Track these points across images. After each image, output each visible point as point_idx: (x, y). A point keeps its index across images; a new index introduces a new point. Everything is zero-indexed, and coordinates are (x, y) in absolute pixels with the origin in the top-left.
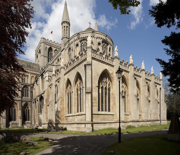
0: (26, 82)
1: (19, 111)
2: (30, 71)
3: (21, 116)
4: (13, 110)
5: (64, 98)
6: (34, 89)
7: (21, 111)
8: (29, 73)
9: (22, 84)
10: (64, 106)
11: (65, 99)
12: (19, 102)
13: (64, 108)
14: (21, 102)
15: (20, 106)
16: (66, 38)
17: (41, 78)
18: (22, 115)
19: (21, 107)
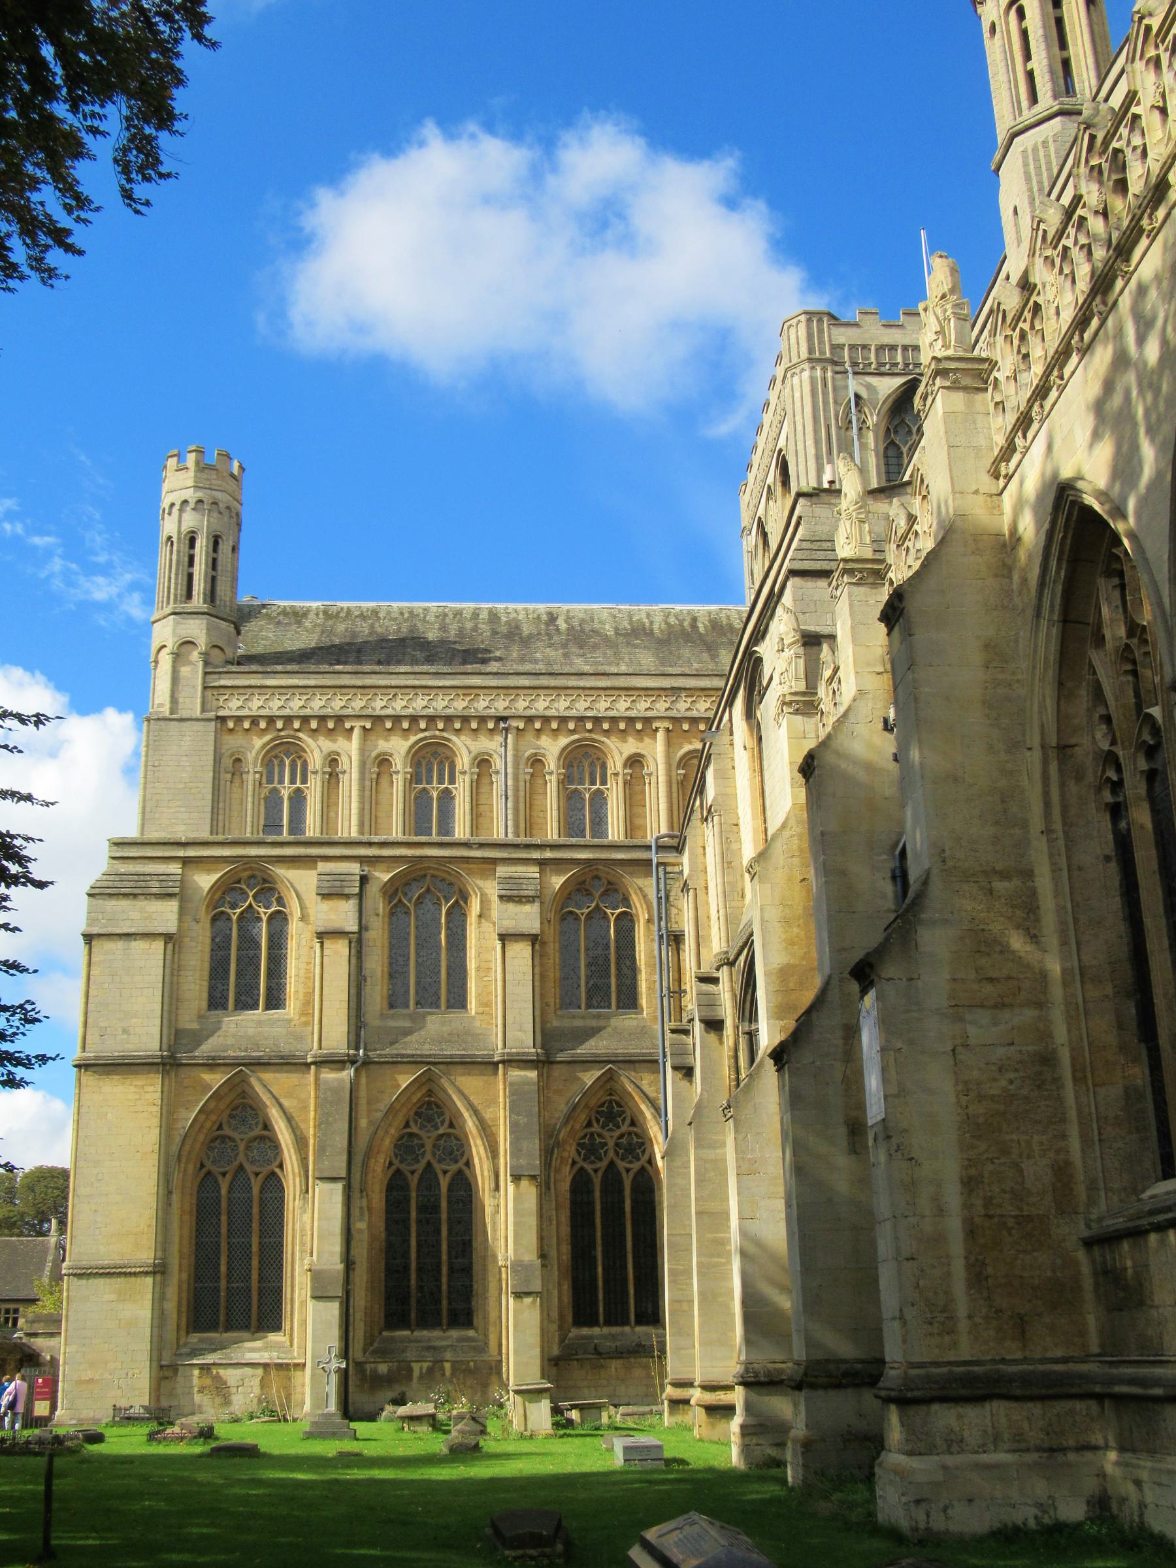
0: (615, 831)
1: (511, 1188)
2: (661, 707)
3: (531, 1256)
4: (444, 1182)
5: (1028, 874)
6: (685, 887)
7: (530, 1191)
8: (647, 721)
9: (542, 863)
10: (1045, 1035)
11: (1044, 882)
12: (516, 1074)
13: (1047, 1059)
14: (533, 1075)
15: (514, 1128)
16: (1058, 119)
17: (750, 714)
18: (543, 1256)
19: (533, 1146)
